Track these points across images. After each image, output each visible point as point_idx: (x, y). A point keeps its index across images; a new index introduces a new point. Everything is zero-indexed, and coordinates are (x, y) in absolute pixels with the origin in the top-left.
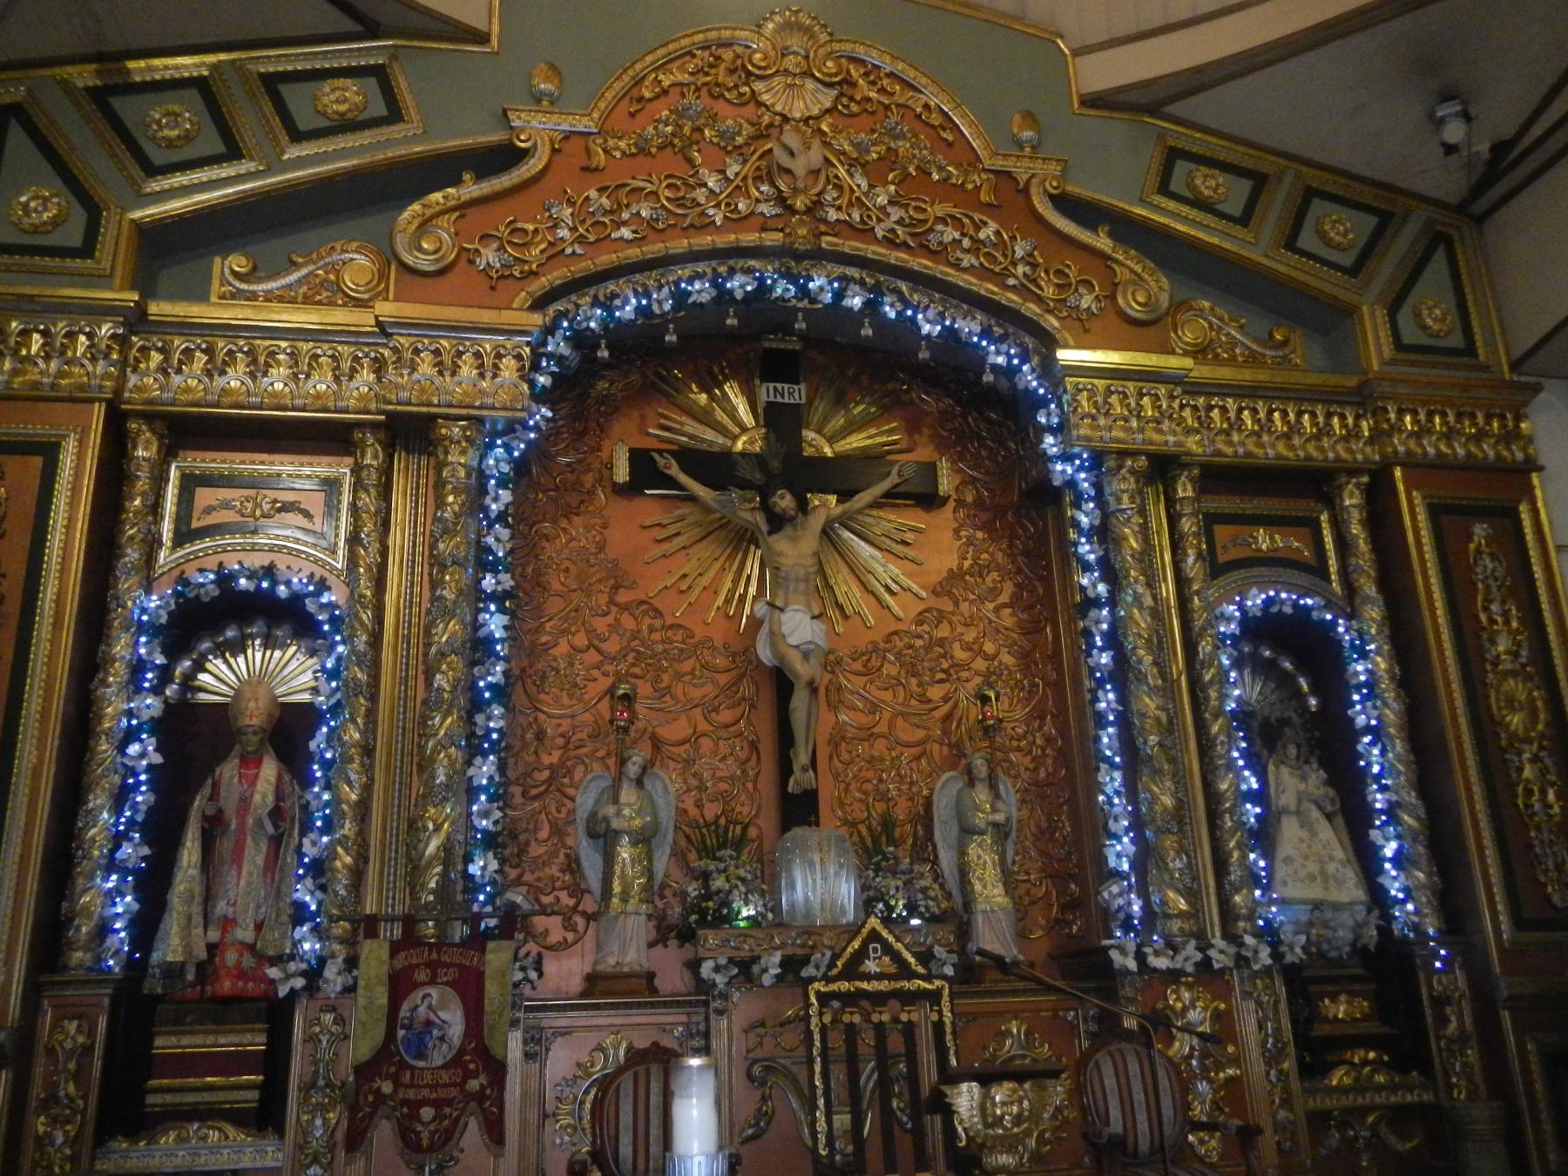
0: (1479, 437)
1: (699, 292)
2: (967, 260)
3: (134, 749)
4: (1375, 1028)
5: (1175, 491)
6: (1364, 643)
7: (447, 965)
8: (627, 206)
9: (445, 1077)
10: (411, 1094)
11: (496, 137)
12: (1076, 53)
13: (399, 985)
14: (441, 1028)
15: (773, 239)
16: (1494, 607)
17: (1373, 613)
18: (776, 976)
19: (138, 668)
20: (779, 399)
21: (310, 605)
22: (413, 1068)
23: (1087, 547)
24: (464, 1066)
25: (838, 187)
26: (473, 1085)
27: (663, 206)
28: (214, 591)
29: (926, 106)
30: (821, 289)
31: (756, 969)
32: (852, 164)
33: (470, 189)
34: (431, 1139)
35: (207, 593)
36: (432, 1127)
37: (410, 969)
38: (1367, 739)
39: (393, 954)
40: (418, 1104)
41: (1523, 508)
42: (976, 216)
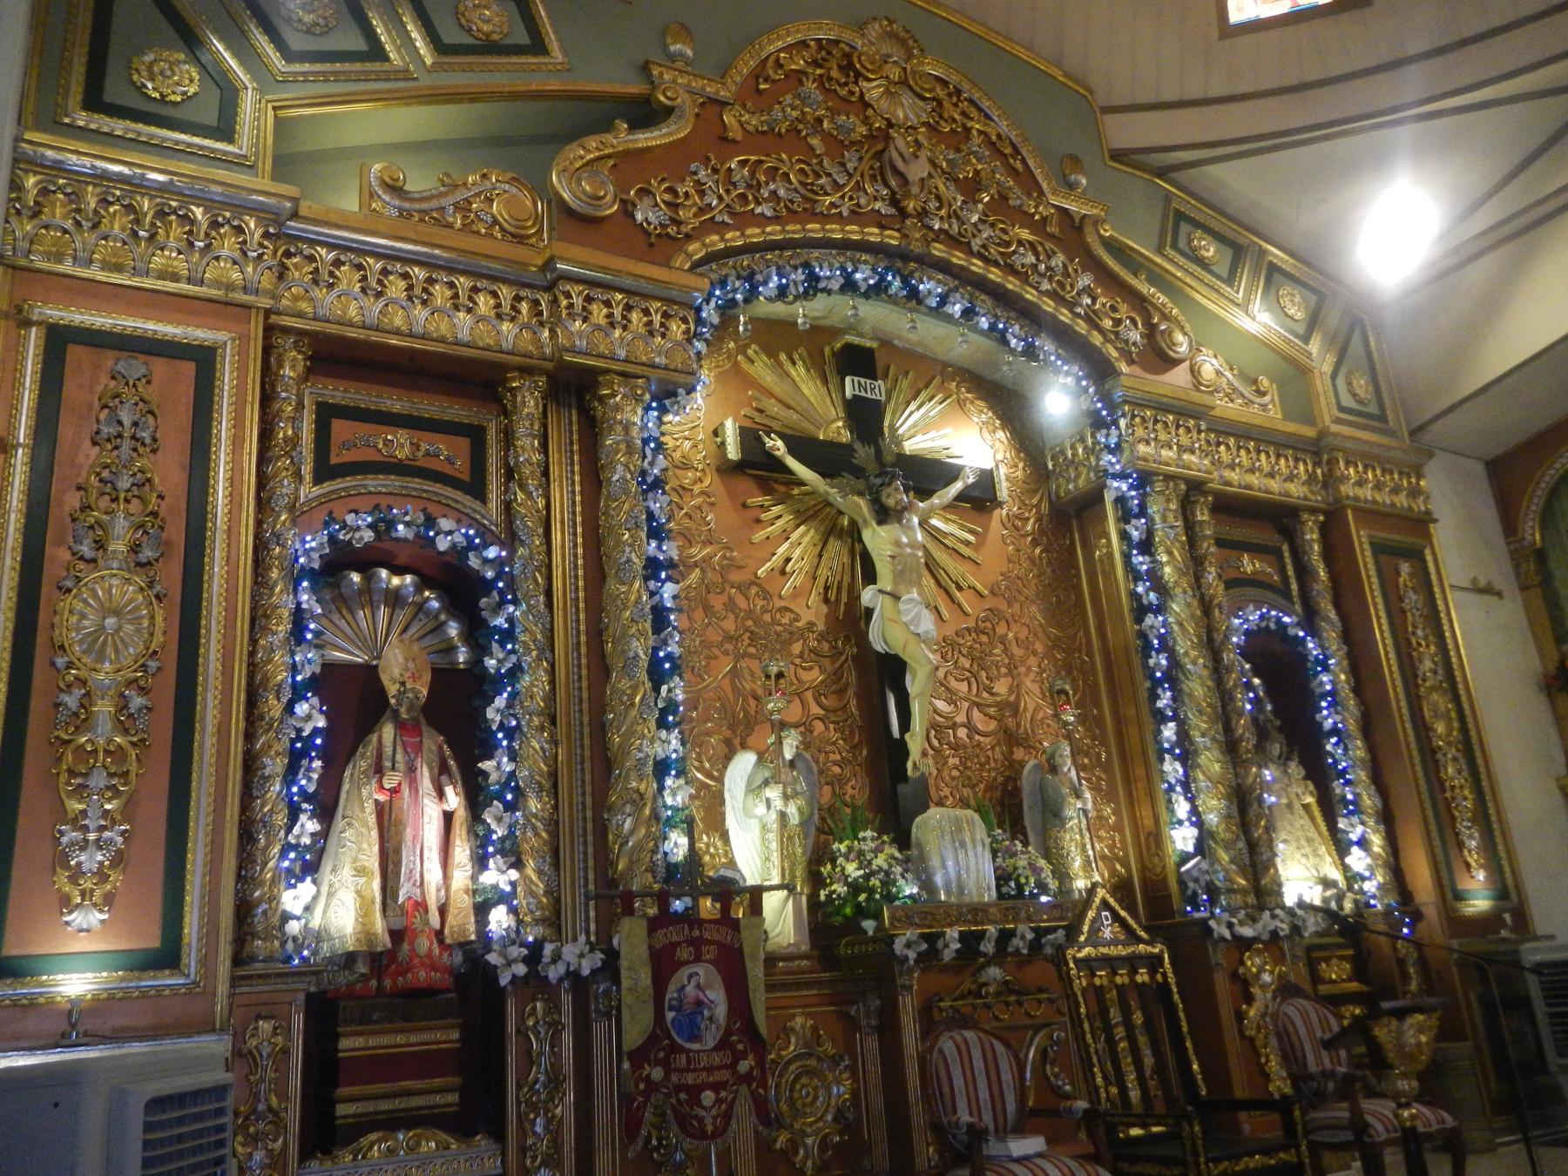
0: (1396, 490)
1: (829, 278)
2: (1046, 286)
3: (302, 708)
4: (1354, 986)
5: (1194, 515)
6: (1327, 658)
7: (710, 942)
8: (767, 183)
9: (717, 1059)
10: (690, 1079)
11: (636, 88)
12: (1107, 110)
13: (663, 965)
14: (710, 1009)
15: (892, 239)
16: (1420, 632)
17: (1332, 636)
18: (957, 951)
19: (299, 617)
20: (863, 394)
21: (474, 562)
22: (688, 1051)
23: (1141, 559)
24: (732, 1047)
25: (938, 198)
26: (744, 1066)
27: (796, 190)
28: (368, 535)
29: (999, 136)
30: (930, 292)
31: (940, 944)
32: (950, 177)
33: (623, 138)
34: (714, 1124)
36: (714, 1112)
37: (673, 946)
38: (1334, 740)
40: (700, 1088)
41: (1428, 552)
42: (1048, 245)
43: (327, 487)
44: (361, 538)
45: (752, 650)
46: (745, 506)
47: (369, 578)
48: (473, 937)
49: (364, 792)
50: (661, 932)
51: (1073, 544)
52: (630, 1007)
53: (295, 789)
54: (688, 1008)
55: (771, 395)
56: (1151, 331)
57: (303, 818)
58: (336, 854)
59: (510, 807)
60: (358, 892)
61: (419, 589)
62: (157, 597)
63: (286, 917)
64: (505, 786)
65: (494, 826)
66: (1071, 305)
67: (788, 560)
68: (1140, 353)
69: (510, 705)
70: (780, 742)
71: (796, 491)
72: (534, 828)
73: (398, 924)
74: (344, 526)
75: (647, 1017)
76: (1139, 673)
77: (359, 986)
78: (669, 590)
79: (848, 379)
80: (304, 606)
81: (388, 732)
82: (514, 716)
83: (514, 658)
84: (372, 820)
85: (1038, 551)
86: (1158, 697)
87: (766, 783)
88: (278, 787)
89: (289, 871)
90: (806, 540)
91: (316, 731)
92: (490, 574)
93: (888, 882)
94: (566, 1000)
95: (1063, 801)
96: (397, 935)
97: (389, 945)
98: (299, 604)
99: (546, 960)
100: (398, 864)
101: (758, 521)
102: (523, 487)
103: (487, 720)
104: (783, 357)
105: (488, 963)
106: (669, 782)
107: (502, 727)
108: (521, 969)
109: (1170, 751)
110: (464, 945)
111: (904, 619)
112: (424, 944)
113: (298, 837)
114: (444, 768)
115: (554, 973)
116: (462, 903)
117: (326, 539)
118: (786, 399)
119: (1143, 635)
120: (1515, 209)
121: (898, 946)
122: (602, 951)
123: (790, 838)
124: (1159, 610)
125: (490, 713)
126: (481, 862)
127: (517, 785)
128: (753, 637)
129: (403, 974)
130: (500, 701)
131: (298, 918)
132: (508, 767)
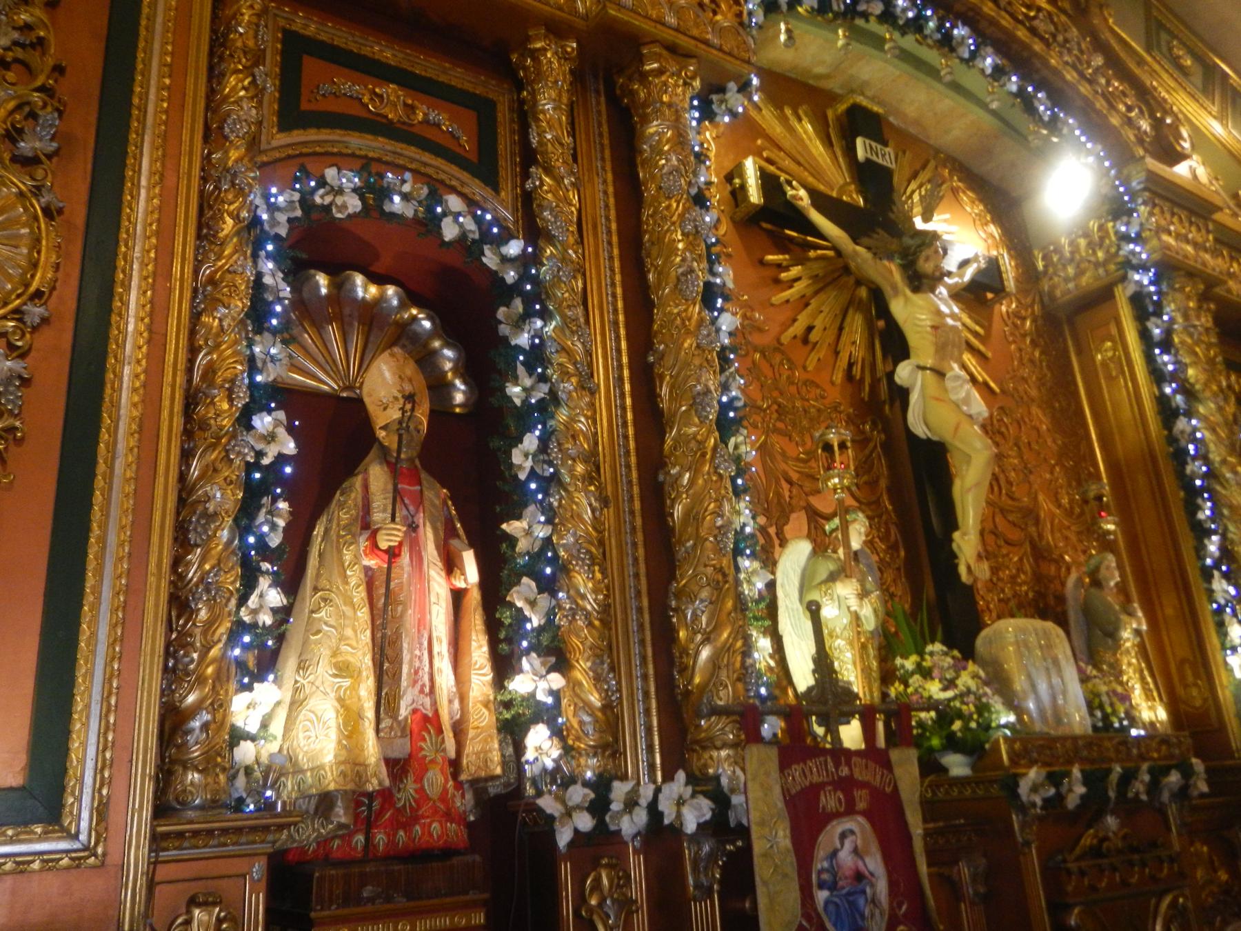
3: (263, 422)
7: (863, 785)
18: (1082, 797)
20: (874, 158)
21: (490, 259)
23: (1166, 358)
35: (344, 206)
37: (814, 791)
39: (784, 765)
42: (1063, 18)
43: (298, 136)
44: (344, 206)
45: (780, 425)
46: (762, 263)
47: (340, 285)
48: (498, 771)
49: (348, 556)
50: (796, 770)
51: (1066, 351)
52: (765, 883)
53: (251, 540)
54: (845, 885)
55: (780, 149)
56: (1158, 124)
57: (264, 583)
58: (306, 642)
59: (548, 586)
60: (340, 700)
61: (403, 306)
62: (47, 211)
63: (237, 736)
64: (537, 557)
65: (527, 613)
66: (1091, 82)
67: (810, 329)
68: (1150, 143)
69: (544, 442)
70: (845, 527)
71: (812, 254)
72: (588, 615)
73: (401, 748)
74: (322, 183)
75: (792, 895)
76: (1169, 482)
77: (337, 843)
78: (727, 322)
79: (859, 141)
80: (268, 280)
81: (377, 476)
82: (550, 464)
83: (545, 388)
84: (360, 595)
85: (1037, 354)
88: (225, 534)
89: (241, 664)
90: (826, 309)
91: (281, 459)
92: (511, 276)
93: (983, 708)
94: (637, 867)
95: (1118, 620)
96: (397, 767)
97: (387, 783)
98: (259, 275)
99: (615, 807)
100: (397, 661)
101: (777, 281)
102: (548, 170)
103: (511, 465)
104: (788, 112)
105: (540, 810)
107: (533, 474)
108: (585, 822)
109: (1217, 565)
110: (478, 785)
111: (953, 397)
112: (436, 780)
113: (255, 612)
114: (451, 532)
115: (630, 825)
116: (483, 720)
117: (297, 196)
118: (794, 152)
119: (1172, 440)
121: (1024, 788)
122: (706, 794)
123: (864, 647)
124: (1189, 414)
125: (517, 457)
126: (503, 666)
127: (556, 556)
128: (781, 412)
129: (407, 826)
130: (531, 441)
131: (253, 738)
132: (542, 532)
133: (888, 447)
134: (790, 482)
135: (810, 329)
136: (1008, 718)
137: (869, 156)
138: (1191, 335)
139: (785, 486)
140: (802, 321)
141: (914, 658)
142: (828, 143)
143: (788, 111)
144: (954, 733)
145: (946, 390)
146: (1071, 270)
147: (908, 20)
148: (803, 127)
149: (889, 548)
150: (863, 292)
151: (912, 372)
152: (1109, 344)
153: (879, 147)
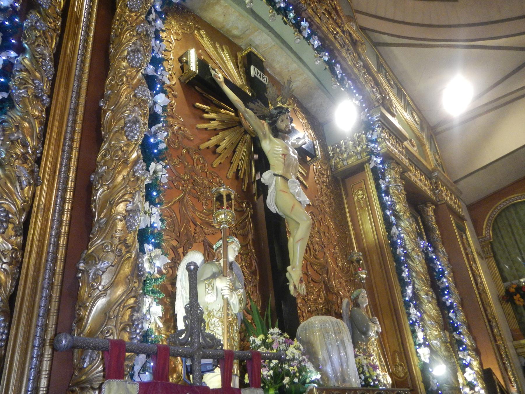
20: (259, 77)
67: (217, 146)
70: (225, 246)
71: (223, 111)
79: (252, 67)
85: (329, 192)
86: (403, 271)
87: (214, 276)
90: (227, 139)
93: (302, 369)
106: (148, 247)
109: (411, 301)
119: (390, 237)
120: (504, 94)
123: (231, 324)
133: (254, 217)
134: (196, 225)
135: (217, 146)
136: (315, 376)
137: (256, 75)
138: (397, 190)
139: (193, 226)
140: (214, 140)
141: (261, 336)
142: (236, 66)
143: (217, 45)
144: (284, 385)
145: (288, 188)
146: (345, 156)
147: (280, 7)
148: (224, 54)
149: (251, 273)
150: (248, 137)
151: (271, 176)
152: (361, 192)
153: (262, 73)
